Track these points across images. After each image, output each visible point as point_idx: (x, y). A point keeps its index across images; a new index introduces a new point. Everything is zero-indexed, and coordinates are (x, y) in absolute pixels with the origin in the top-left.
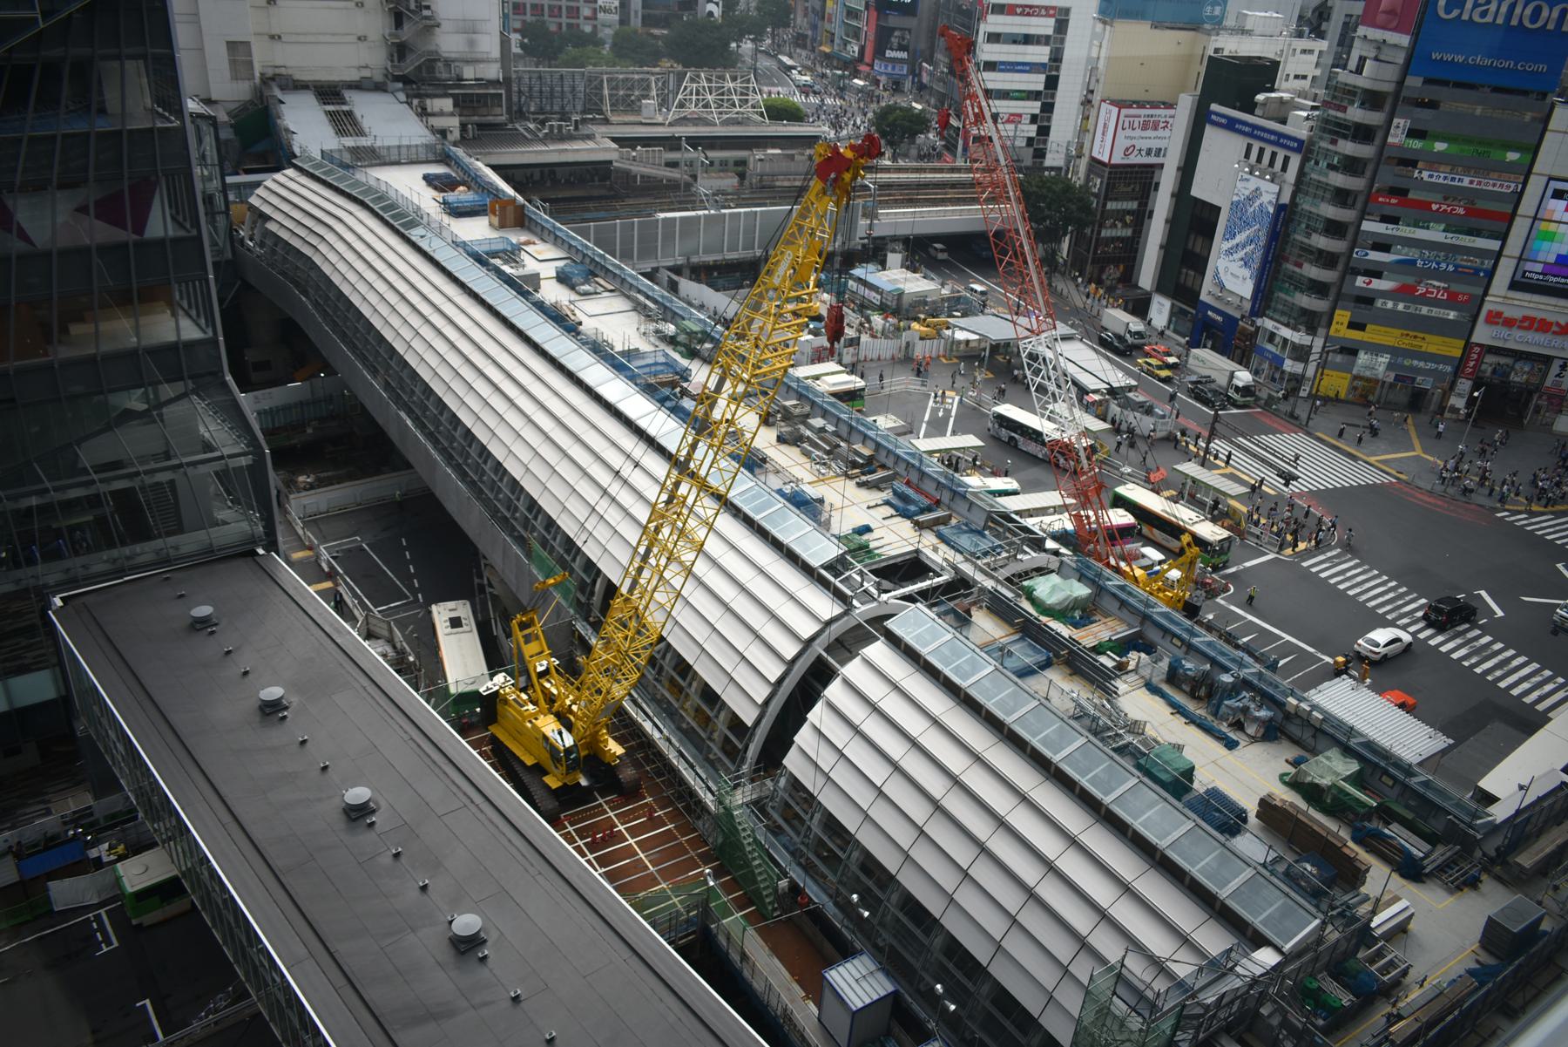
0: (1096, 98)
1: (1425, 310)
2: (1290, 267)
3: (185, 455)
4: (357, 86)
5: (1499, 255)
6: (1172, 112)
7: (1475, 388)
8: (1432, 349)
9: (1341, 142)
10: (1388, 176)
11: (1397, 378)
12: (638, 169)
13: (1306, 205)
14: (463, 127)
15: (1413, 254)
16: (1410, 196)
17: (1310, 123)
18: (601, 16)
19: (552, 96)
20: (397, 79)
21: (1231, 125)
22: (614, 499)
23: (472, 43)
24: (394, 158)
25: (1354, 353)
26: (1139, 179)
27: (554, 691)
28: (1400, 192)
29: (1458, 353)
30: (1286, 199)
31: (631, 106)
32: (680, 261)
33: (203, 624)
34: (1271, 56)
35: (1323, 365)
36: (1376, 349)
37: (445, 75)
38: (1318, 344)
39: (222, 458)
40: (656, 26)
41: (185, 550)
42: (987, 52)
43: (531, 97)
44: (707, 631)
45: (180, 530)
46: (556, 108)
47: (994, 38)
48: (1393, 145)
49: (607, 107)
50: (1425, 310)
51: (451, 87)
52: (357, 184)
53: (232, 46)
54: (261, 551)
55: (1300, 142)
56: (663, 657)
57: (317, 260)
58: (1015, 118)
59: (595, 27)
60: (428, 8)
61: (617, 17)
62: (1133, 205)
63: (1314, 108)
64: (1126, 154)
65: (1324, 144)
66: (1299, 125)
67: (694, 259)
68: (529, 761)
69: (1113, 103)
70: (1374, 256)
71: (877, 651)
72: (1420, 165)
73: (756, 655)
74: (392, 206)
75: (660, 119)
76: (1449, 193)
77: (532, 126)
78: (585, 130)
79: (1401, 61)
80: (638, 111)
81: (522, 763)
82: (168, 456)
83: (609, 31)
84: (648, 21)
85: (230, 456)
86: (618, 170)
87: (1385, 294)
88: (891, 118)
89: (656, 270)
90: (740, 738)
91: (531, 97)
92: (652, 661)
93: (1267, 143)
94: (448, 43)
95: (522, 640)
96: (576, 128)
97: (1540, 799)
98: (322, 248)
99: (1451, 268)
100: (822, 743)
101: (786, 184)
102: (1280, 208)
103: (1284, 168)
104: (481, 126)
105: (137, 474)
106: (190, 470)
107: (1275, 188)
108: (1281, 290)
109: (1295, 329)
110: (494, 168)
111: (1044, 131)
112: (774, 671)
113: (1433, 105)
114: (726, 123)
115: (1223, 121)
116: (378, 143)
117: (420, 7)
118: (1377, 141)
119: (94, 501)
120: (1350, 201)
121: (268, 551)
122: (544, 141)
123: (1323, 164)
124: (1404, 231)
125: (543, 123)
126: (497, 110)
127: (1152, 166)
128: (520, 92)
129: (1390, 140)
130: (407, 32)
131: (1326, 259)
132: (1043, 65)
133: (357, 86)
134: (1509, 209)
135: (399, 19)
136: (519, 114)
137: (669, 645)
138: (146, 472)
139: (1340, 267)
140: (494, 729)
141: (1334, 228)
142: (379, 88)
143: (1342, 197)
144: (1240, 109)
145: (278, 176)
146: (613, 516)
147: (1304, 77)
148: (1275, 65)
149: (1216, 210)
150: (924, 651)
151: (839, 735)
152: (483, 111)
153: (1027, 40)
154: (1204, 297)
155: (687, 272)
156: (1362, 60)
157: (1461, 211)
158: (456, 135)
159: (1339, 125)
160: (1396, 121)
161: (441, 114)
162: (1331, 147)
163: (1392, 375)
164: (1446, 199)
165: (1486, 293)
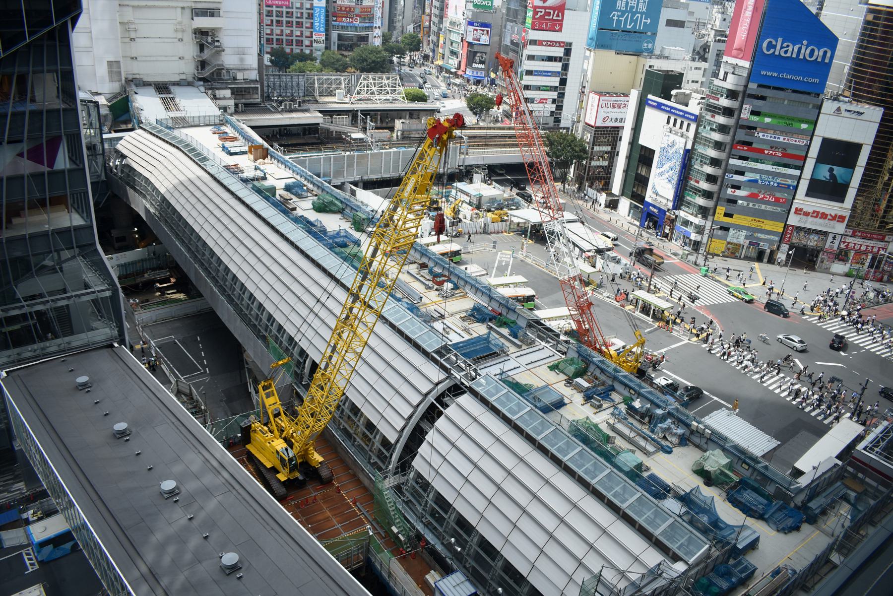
0: (586, 91)
1: (763, 207)
2: (692, 182)
3: (73, 291)
4: (177, 84)
5: (800, 177)
6: (626, 99)
7: (790, 249)
8: (768, 228)
9: (717, 116)
10: (742, 135)
11: (750, 243)
12: (333, 128)
13: (700, 149)
14: (236, 105)
15: (757, 177)
16: (754, 146)
17: (700, 107)
18: (315, 45)
19: (286, 88)
21: (659, 107)
22: (317, 315)
23: (242, 60)
24: (197, 123)
25: (727, 229)
26: (610, 135)
27: (283, 425)
28: (749, 144)
29: (781, 230)
30: (689, 147)
32: (357, 178)
33: (84, 385)
34: (679, 70)
35: (711, 237)
36: (739, 228)
37: (226, 77)
38: (708, 224)
39: (94, 292)
41: (74, 344)
42: (528, 65)
43: (274, 89)
44: (368, 389)
45: (72, 333)
46: (289, 95)
47: (531, 58)
48: (744, 119)
49: (317, 94)
50: (763, 207)
51: (230, 83)
52: (174, 138)
54: (116, 345)
55: (696, 116)
56: (344, 404)
57: (152, 180)
58: (543, 101)
60: (218, 41)
61: (324, 46)
62: (608, 148)
63: (702, 98)
64: (604, 120)
65: (708, 117)
66: (694, 107)
67: (365, 178)
68: (269, 465)
69: (596, 93)
70: (737, 177)
71: (465, 400)
72: (758, 129)
73: (397, 402)
74: (194, 150)
75: (347, 100)
76: (774, 146)
77: (275, 105)
78: (304, 107)
79: (745, 75)
81: (265, 466)
82: (65, 291)
83: (319, 53)
85: (99, 291)
86: (322, 129)
87: (742, 198)
88: (475, 100)
89: (343, 183)
90: (388, 450)
91: (274, 89)
92: (338, 407)
93: (677, 117)
94: (229, 60)
95: (264, 396)
96: (299, 105)
97: (824, 474)
98: (156, 173)
99: (776, 185)
100: (433, 451)
102: (687, 151)
103: (687, 130)
104: (246, 105)
105: (47, 302)
106: (77, 300)
107: (683, 140)
108: (688, 195)
109: (696, 216)
110: (253, 128)
111: (560, 108)
112: (407, 411)
113: (763, 98)
115: (655, 104)
116: (188, 115)
117: (214, 41)
118: (735, 116)
119: (24, 317)
120: (723, 148)
121: (120, 345)
123: (708, 128)
124: (751, 164)
125: (281, 103)
126: (256, 96)
127: (617, 127)
128: (268, 86)
129: (742, 116)
130: (207, 54)
131: (711, 179)
132: (558, 72)
133: (177, 84)
134: (804, 154)
135: (202, 48)
136: (268, 98)
137: (347, 397)
138: (52, 301)
139: (719, 183)
140: (248, 447)
141: (715, 162)
142: (190, 84)
143: (718, 145)
144: (664, 98)
145: (131, 133)
146: (316, 324)
147: (697, 82)
148: (681, 75)
149: (652, 152)
150: (491, 400)
151: (443, 446)
152: (248, 96)
153: (550, 59)
154: (647, 199)
155: (361, 184)
156: (726, 74)
157: (780, 154)
158: (232, 109)
159: (715, 107)
160: (744, 106)
162: (712, 119)
163: (748, 242)
164: (772, 148)
165: (794, 198)
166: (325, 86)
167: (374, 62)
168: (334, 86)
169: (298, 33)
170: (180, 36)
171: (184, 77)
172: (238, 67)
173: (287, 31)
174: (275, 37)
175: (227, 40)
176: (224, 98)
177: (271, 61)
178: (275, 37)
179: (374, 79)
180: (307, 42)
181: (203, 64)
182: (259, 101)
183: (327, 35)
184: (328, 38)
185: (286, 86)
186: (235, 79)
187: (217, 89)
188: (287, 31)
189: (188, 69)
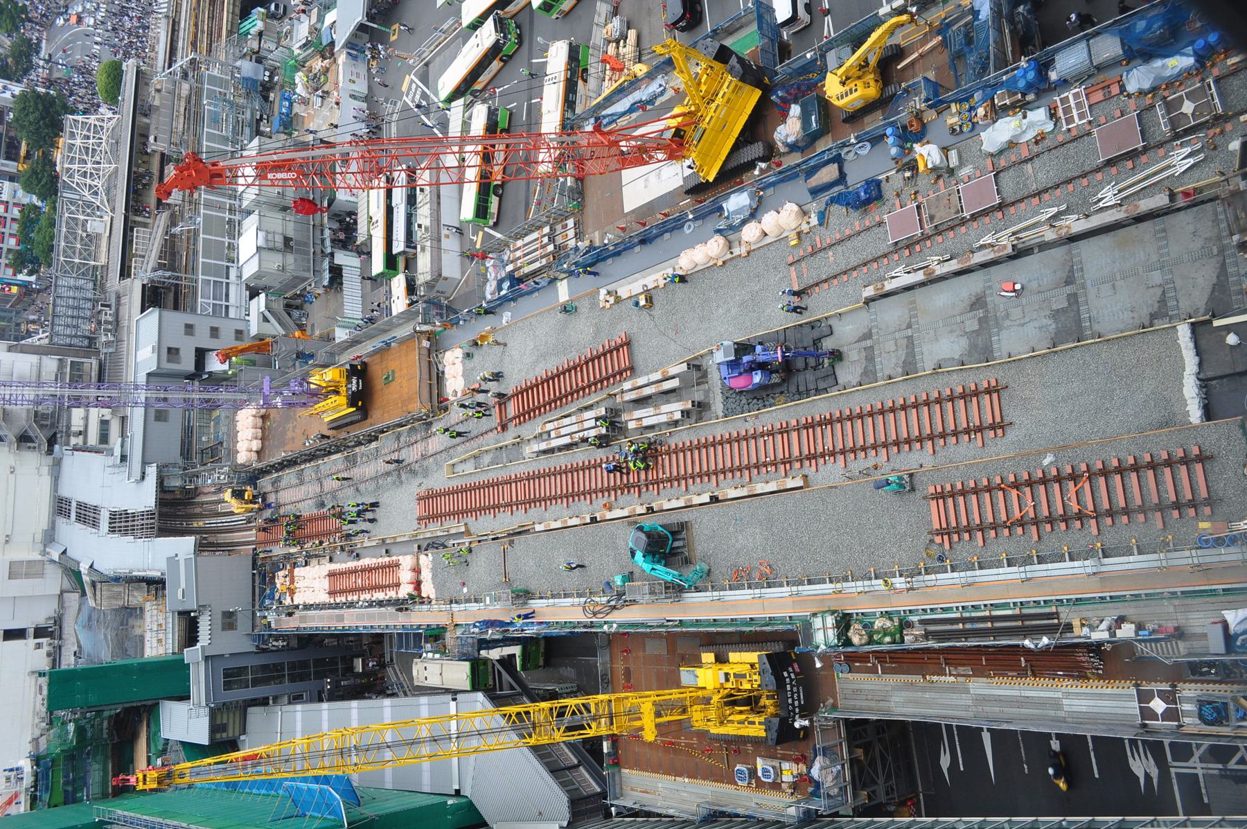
14: (99, 403)
19: (78, 308)
20: (50, 451)
31: (92, 239)
40: (18, 148)
43: (76, 327)
46: (89, 305)
59: (15, 205)
75: (107, 219)
80: (98, 236)
83: (20, 193)
101: (181, 120)
122: (119, 340)
126: (87, 367)
133: (56, 490)
142: (57, 465)
158: (107, 413)
161: (86, 419)
166: (79, 246)
167: (43, 118)
171: (45, 470)
176: (86, 419)
177: (30, 273)
179: (72, 161)
181: (24, 439)
182: (95, 362)
185: (74, 308)
187: (68, 427)
189: (33, 464)
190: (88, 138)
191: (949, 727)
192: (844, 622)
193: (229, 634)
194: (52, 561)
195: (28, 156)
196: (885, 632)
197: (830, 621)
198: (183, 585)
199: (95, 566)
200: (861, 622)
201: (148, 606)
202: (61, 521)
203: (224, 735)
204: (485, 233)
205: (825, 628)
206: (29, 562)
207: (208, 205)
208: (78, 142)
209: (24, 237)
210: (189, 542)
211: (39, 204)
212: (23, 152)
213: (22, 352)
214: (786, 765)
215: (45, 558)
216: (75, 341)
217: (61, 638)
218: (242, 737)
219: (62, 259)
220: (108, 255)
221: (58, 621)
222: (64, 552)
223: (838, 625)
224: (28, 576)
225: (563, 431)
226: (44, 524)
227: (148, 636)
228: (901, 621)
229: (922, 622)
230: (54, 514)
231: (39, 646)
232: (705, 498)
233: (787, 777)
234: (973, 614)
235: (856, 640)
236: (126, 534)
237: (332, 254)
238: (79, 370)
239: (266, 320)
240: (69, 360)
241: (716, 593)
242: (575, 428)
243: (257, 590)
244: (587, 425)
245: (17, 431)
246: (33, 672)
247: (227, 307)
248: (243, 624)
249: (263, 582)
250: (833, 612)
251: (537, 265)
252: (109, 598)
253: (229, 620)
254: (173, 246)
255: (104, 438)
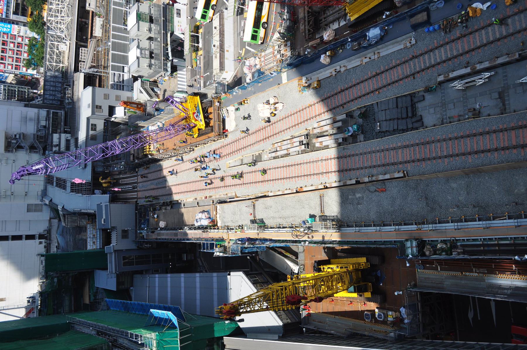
14: (65, 132)
18: (21, 34)
20: (44, 154)
23: (31, 120)
37: (44, 132)
43: (55, 95)
46: (60, 85)
53: (28, 211)
60: (15, 135)
61: (22, 27)
75: (68, 43)
83: (29, 31)
84: (24, 14)
91: (55, 95)
94: (31, 129)
114: (73, 15)
117: (15, 138)
135: (20, 147)
158: (68, 135)
166: (55, 57)
168: (55, 50)
169: (12, 45)
170: (12, 161)
172: (36, 123)
173: (10, 54)
174: (14, 63)
175: (16, 128)
178: (14, 63)
180: (19, 40)
181: (32, 148)
182: (63, 112)
183: (13, 23)
184: (17, 23)
186: (45, 127)
187: (52, 142)
188: (10, 54)
190: (59, 5)
191: (474, 298)
192: (422, 244)
193: (125, 240)
194: (46, 204)
195: (32, 14)
196: (442, 250)
197: (414, 243)
198: (104, 217)
199: (65, 207)
200: (430, 245)
201: (88, 226)
202: (49, 187)
203: (123, 287)
204: (246, 50)
205: (412, 247)
206: (36, 205)
207: (114, 37)
208: (54, 7)
209: (30, 52)
210: (107, 197)
211: (36, 36)
212: (29, 13)
213: (31, 107)
214: (390, 313)
215: (42, 203)
216: (54, 102)
217: (50, 240)
218: (131, 288)
219: (48, 63)
220: (68, 62)
221: (49, 231)
222: (51, 200)
223: (418, 246)
224: (35, 211)
225: (283, 148)
226: (42, 187)
227: (89, 240)
228: (451, 245)
229: (461, 245)
230: (46, 183)
231: (41, 243)
232: (354, 182)
233: (390, 319)
234: (489, 243)
235: (427, 253)
236: (78, 193)
237: (172, 60)
238: (57, 116)
239: (141, 92)
240: (52, 111)
241: (357, 228)
242: (289, 146)
243: (138, 221)
244: (295, 144)
245: (29, 144)
246: (38, 255)
247: (123, 86)
248: (131, 236)
249: (140, 216)
250: (416, 240)
251: (272, 65)
252: (71, 222)
253: (125, 234)
254: (98, 57)
255: (68, 148)
